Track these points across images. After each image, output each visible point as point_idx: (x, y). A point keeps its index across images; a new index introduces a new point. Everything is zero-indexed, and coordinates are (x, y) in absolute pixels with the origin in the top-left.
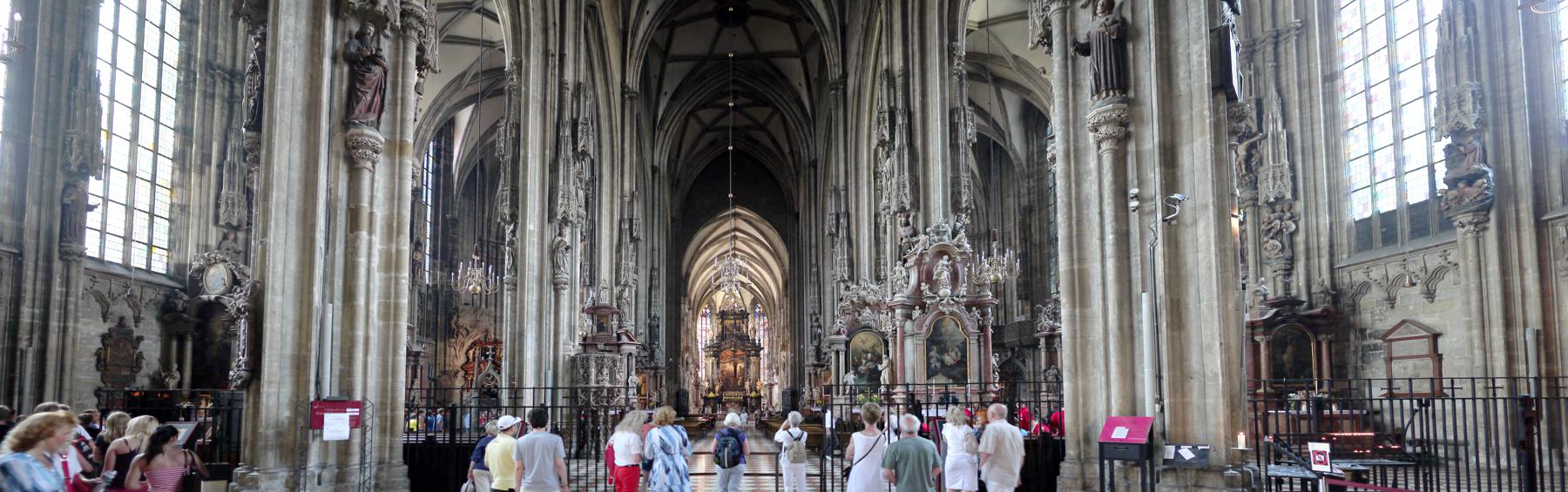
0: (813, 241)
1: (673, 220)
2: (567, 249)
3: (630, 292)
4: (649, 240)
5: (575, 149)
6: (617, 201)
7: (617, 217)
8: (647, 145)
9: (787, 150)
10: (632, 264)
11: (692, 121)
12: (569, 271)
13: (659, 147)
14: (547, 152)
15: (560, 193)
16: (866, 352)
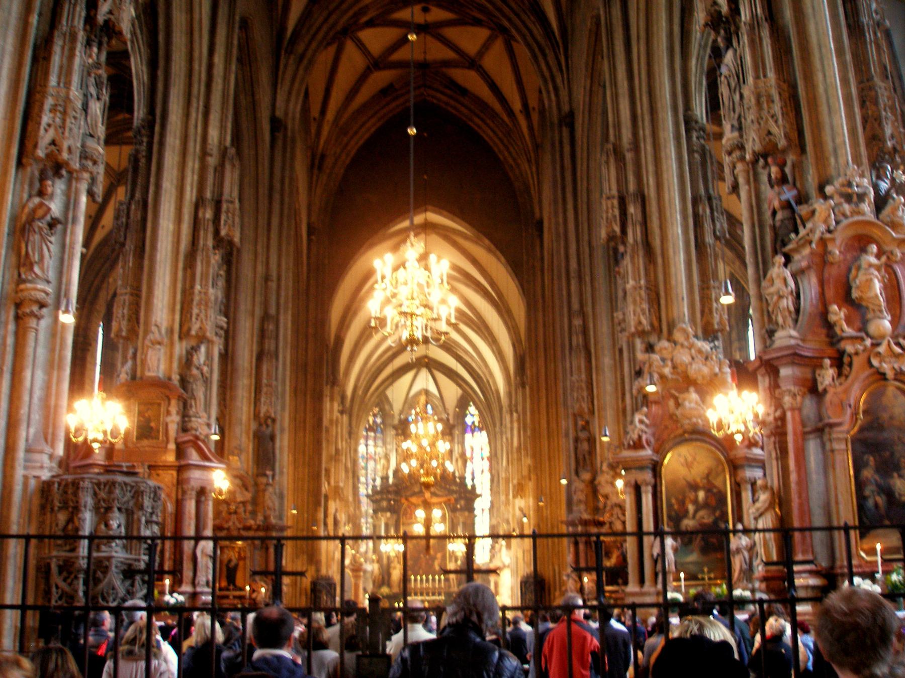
0: (573, 264)
1: (311, 230)
2: (52, 225)
3: (209, 356)
4: (261, 258)
5: (90, 20)
6: (193, 165)
7: (190, 195)
8: (264, 76)
9: (517, 106)
10: (215, 293)
11: (350, 47)
12: (52, 275)
13: (286, 88)
14: (34, 19)
15: (49, 102)
16: (694, 487)
